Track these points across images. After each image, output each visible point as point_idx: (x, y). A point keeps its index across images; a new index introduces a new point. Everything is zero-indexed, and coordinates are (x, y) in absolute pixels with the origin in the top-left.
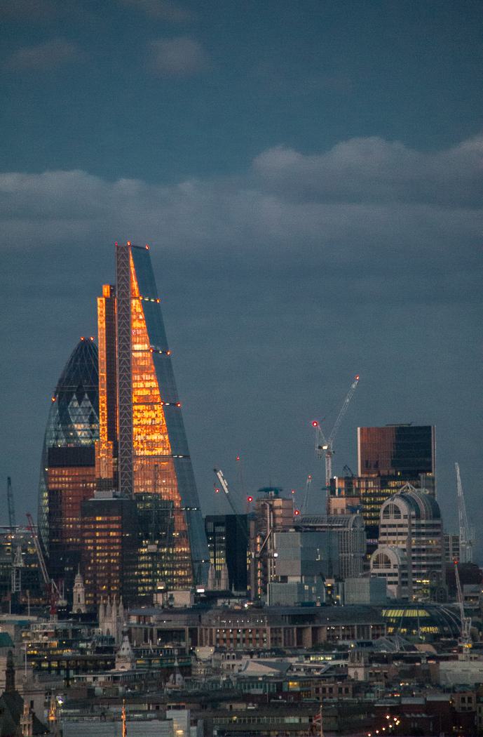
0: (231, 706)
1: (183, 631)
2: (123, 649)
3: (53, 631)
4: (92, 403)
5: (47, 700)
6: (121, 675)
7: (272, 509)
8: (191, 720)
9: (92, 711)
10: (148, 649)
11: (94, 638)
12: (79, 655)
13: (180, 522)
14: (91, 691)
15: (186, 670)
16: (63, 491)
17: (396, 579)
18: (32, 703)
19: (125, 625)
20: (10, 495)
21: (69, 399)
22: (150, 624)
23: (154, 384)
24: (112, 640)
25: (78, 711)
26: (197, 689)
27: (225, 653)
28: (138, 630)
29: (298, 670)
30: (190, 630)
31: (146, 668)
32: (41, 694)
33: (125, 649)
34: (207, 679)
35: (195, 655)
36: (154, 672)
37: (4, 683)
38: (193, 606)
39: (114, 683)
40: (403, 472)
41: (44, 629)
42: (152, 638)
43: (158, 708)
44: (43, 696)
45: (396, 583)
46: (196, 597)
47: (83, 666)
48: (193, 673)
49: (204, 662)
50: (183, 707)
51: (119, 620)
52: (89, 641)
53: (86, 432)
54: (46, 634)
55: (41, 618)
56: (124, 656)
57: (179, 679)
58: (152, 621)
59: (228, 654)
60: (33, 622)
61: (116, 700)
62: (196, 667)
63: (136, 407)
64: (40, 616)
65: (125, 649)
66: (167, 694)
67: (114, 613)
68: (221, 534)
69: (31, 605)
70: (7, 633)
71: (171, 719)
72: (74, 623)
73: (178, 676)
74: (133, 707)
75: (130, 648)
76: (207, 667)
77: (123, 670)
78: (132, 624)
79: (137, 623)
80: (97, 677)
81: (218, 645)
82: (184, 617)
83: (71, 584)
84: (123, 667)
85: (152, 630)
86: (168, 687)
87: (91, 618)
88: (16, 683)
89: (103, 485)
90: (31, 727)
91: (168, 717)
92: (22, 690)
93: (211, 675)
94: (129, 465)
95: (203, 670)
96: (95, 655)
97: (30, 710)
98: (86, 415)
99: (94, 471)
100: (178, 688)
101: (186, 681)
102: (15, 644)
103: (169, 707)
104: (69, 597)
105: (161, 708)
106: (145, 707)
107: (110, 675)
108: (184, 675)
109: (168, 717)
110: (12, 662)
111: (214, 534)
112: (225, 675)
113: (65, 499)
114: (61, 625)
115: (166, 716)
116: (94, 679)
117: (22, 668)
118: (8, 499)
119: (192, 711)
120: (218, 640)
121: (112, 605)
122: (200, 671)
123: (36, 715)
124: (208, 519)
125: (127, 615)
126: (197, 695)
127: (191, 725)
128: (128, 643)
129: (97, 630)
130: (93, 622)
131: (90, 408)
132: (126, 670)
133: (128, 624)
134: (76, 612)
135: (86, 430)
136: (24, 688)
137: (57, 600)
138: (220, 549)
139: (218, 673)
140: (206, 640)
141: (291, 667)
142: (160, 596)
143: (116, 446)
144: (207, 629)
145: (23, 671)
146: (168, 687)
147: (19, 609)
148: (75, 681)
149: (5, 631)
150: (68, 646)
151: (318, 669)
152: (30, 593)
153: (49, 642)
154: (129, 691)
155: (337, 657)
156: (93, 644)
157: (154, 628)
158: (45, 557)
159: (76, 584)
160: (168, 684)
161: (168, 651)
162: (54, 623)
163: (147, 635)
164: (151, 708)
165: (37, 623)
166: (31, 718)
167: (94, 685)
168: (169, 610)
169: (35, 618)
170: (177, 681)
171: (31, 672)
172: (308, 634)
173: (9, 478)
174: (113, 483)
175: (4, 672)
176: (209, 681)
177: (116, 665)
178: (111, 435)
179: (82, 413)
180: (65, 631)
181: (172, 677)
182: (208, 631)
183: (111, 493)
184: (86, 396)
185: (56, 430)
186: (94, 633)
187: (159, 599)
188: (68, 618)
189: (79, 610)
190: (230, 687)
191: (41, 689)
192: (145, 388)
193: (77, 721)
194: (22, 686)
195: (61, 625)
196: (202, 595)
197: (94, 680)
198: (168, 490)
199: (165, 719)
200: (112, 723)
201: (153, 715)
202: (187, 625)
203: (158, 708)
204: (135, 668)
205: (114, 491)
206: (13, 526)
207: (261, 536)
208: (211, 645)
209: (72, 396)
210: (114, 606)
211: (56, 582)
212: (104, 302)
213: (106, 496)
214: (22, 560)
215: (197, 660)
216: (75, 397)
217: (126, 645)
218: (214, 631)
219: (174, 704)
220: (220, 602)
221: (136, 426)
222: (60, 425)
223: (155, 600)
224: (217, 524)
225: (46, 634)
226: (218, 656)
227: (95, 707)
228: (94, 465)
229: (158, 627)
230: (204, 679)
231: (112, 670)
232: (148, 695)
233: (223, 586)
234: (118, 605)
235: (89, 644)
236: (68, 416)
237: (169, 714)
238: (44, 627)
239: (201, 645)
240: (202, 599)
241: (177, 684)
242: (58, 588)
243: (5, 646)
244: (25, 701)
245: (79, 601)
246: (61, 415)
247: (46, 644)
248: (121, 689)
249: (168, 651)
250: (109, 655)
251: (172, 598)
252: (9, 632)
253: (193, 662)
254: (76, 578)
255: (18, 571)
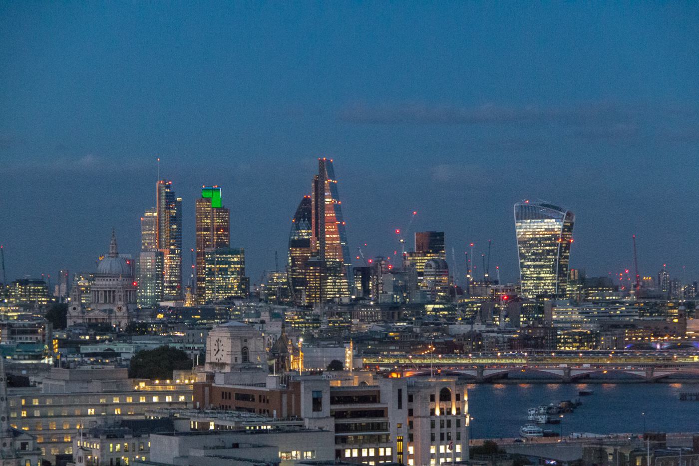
7: (381, 265)
17: (430, 293)
18: (292, 340)
29: (393, 328)
40: (433, 251)
45: (430, 294)
51: (321, 308)
56: (324, 323)
63: (327, 224)
103: (344, 343)
106: (334, 342)
141: (390, 327)
142: (337, 299)
151: (401, 328)
155: (409, 324)
169: (287, 307)
172: (396, 315)
199: (343, 347)
201: (338, 346)
207: (376, 276)
220: (361, 302)
224: (358, 271)
236: (299, 227)
237: (345, 345)
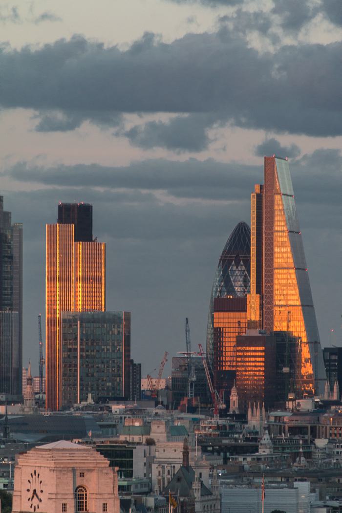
0: (339, 480)
1: (307, 428)
2: (264, 439)
3: (216, 425)
4: (245, 267)
5: (211, 473)
6: (262, 457)
8: (311, 489)
9: (242, 481)
10: (282, 439)
11: (244, 431)
12: (234, 442)
13: (305, 352)
14: (242, 468)
15: (308, 455)
16: (224, 329)
18: (201, 474)
19: (266, 422)
20: (187, 331)
21: (230, 264)
22: (283, 422)
23: (290, 255)
24: (257, 433)
25: (232, 481)
26: (315, 468)
27: (336, 443)
28: (275, 427)
30: (312, 427)
31: (281, 452)
32: (207, 468)
33: (266, 439)
34: (323, 461)
35: (315, 444)
36: (286, 455)
37: (182, 460)
38: (314, 410)
39: (258, 462)
41: (209, 424)
42: (284, 433)
43: (288, 480)
44: (208, 470)
46: (316, 404)
47: (238, 450)
48: (313, 457)
49: (321, 449)
50: (306, 480)
51: (261, 419)
52: (241, 433)
53: (241, 288)
54: (210, 427)
55: (208, 417)
56: (265, 444)
57: (303, 461)
58: (285, 420)
59: (338, 444)
60: (202, 419)
61: (258, 474)
62: (315, 453)
63: (276, 271)
64: (207, 415)
65: (266, 439)
66: (295, 471)
67: (258, 414)
68: (334, 361)
69: (201, 408)
70: (184, 426)
71: (297, 488)
72: (230, 420)
73: (302, 459)
74: (270, 479)
75: (269, 438)
76: (323, 453)
77: (264, 453)
78: (271, 422)
79: (274, 422)
80: (246, 458)
81: (331, 438)
82: (308, 418)
83: (228, 394)
84: (264, 451)
85: (284, 427)
86: (295, 467)
87: (242, 418)
88: (190, 460)
89: (251, 325)
90: (200, 490)
91: (294, 487)
92: (194, 465)
93: (325, 459)
94: (271, 317)
95: (320, 455)
96: (245, 443)
97: (199, 479)
98: (241, 276)
99: (246, 315)
100: (302, 467)
101: (308, 462)
102: (189, 433)
103: (296, 480)
104: (227, 402)
105: (290, 480)
106: (279, 479)
107: (255, 457)
108: (306, 458)
109: (294, 487)
110: (187, 446)
111: (329, 361)
112: (335, 459)
113: (225, 334)
114: (221, 422)
115: (293, 486)
116: (244, 459)
117: (194, 450)
118: (186, 334)
119: (311, 482)
120: (331, 435)
121: (257, 408)
122: (318, 455)
123: (203, 482)
124: (326, 350)
125: (267, 416)
126: (314, 472)
127: (311, 492)
128: (268, 435)
129: (246, 426)
130: (244, 420)
131: (244, 271)
132: (266, 454)
133: (268, 422)
134: (232, 413)
135: (241, 286)
136: (195, 464)
137: (219, 404)
138: (334, 370)
139: (330, 458)
140: (323, 434)
142: (290, 403)
143: (261, 298)
144: (323, 427)
145: (193, 453)
146: (295, 467)
147: (192, 410)
148: (231, 460)
149: (183, 425)
150: (227, 435)
152: (200, 399)
153: (213, 433)
154: (268, 468)
156: (243, 435)
157: (286, 425)
158: (211, 374)
159: (232, 394)
160: (295, 464)
161: (296, 441)
162: (217, 420)
163: (281, 430)
164: (283, 480)
165: (205, 420)
166: (200, 485)
167: (243, 463)
168: (296, 413)
169: (203, 417)
170: (301, 462)
171: (200, 453)
173: (187, 319)
174: (261, 324)
175: (182, 453)
176: (324, 463)
177: (260, 450)
178: (259, 291)
179: (238, 275)
180: (224, 426)
181: (298, 459)
182: (324, 428)
183: (258, 330)
184: (242, 263)
185: (220, 286)
186: (244, 428)
187: (290, 405)
188: (226, 417)
189: (234, 412)
190: (339, 467)
191: (207, 465)
192: (283, 257)
193: (232, 488)
194: (193, 463)
195: (221, 422)
196: (320, 403)
197: (244, 460)
198: (298, 328)
199: (293, 488)
200: (255, 490)
201: (285, 485)
202: (309, 424)
203: (288, 480)
204: (272, 453)
205: (260, 329)
206: (189, 352)
208: (326, 438)
209: (232, 262)
210: (259, 410)
211: (219, 392)
212: (256, 197)
213: (255, 333)
214: (195, 377)
215: (316, 448)
216: (233, 262)
217: (266, 437)
218: (328, 428)
219: (300, 478)
220: (333, 408)
221: (277, 285)
222: (223, 283)
223: (287, 406)
224: (331, 354)
225: (210, 427)
226: (332, 446)
227: (244, 479)
228: (246, 311)
229: (289, 425)
230: (320, 461)
231: (257, 454)
232: (281, 471)
233: (335, 397)
234: (261, 409)
235: (241, 436)
237: (296, 484)
238: (210, 423)
239: (319, 438)
240: (320, 406)
241: (301, 464)
242: (220, 396)
243: (182, 435)
244: (196, 473)
245: (234, 405)
246: (223, 275)
247: (210, 434)
248: (262, 466)
249: (296, 441)
250: (255, 443)
251: (299, 405)
252: (185, 426)
253: (313, 450)
254: (232, 389)
255: (192, 384)
